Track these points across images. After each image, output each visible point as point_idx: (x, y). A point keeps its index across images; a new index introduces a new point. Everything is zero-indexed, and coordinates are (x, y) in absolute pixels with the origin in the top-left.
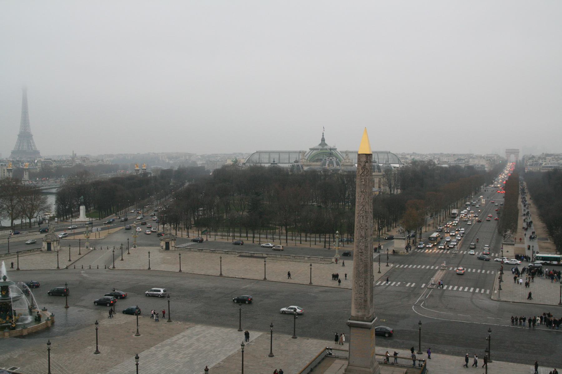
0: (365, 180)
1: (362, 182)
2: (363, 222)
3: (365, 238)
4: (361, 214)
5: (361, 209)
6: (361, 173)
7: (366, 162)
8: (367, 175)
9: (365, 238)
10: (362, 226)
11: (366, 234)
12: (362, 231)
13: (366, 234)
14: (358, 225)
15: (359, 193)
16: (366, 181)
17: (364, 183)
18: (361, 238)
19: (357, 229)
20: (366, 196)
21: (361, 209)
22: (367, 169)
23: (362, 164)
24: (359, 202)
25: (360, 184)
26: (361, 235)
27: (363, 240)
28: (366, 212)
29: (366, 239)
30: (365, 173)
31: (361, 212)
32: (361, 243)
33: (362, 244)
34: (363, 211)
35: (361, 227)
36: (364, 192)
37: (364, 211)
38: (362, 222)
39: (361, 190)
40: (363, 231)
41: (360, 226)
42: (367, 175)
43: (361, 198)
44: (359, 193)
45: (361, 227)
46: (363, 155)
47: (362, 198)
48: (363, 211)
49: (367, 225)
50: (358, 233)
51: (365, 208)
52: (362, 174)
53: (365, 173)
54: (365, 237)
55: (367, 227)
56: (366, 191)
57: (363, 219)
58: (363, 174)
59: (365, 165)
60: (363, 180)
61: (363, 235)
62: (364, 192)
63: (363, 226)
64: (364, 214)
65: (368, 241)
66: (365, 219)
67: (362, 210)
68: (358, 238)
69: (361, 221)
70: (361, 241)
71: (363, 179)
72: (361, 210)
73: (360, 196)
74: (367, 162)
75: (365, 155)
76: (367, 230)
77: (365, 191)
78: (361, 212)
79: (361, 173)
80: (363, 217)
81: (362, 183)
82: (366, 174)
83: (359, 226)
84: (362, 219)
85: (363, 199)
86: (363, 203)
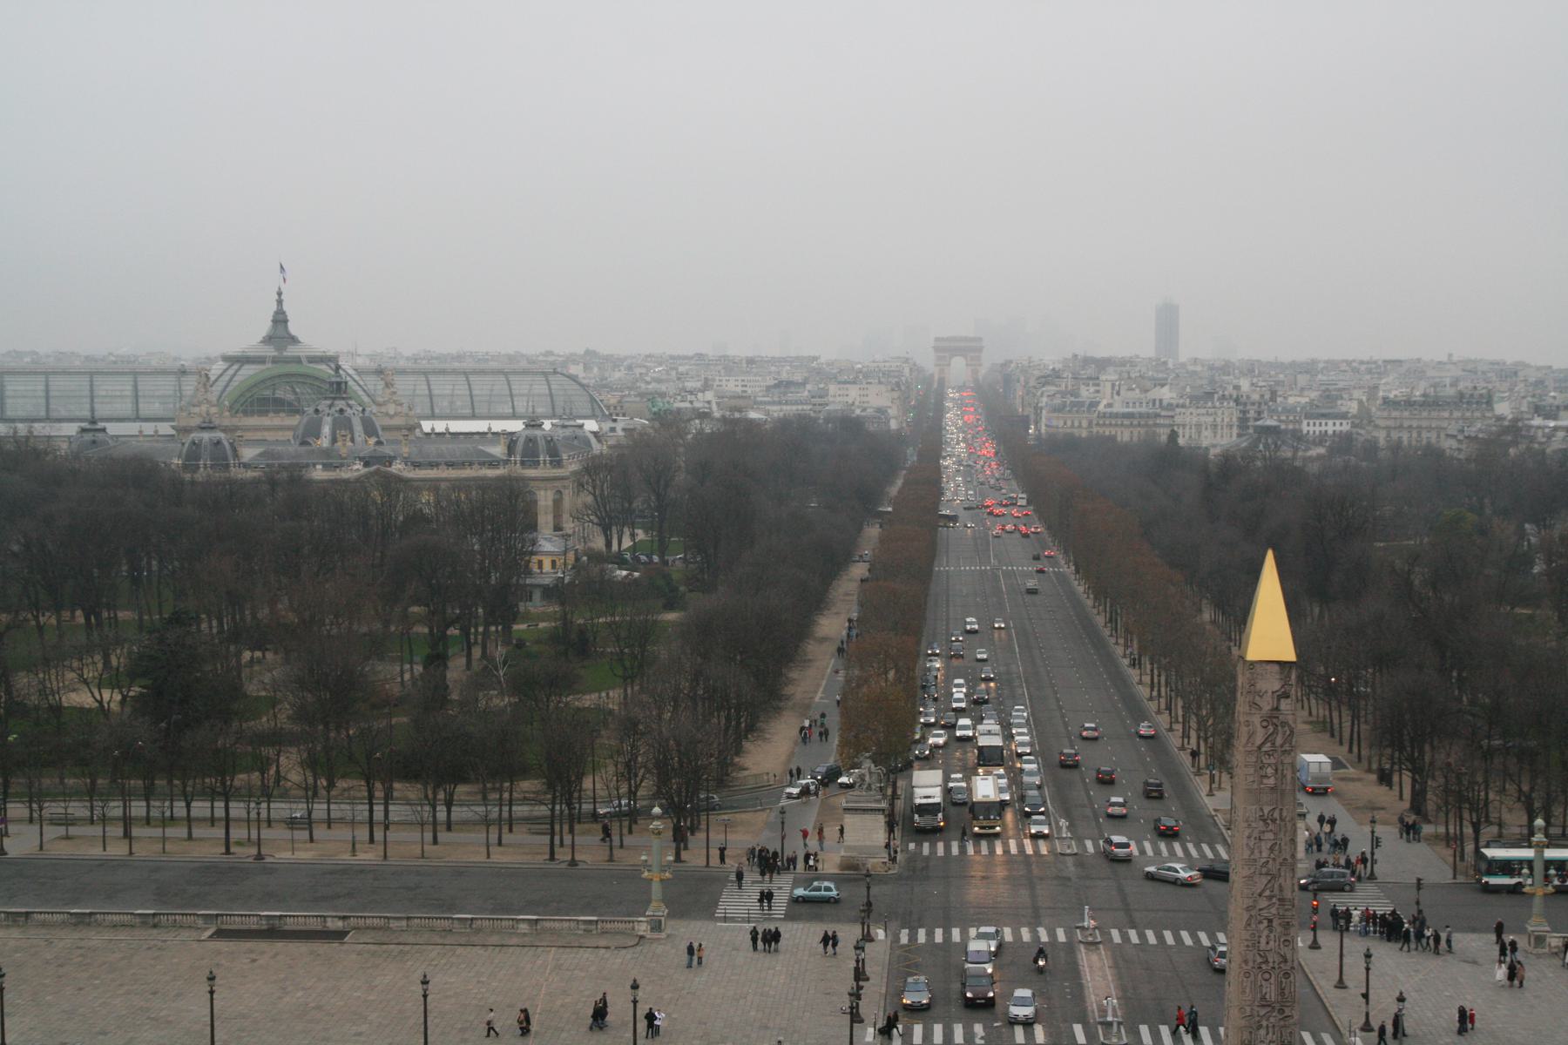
0: (1276, 770)
1: (1266, 776)
2: (1272, 943)
3: (1281, 1011)
4: (1260, 910)
5: (1263, 891)
6: (1259, 740)
7: (1279, 698)
8: (1287, 747)
9: (1281, 1011)
10: (1267, 962)
11: (1282, 994)
12: (1266, 980)
13: (1282, 994)
14: (1250, 957)
15: (1254, 825)
16: (1284, 776)
17: (1271, 781)
18: (1263, 1012)
19: (1247, 974)
20: (1282, 835)
21: (1263, 891)
22: (1284, 724)
23: (1266, 705)
24: (1255, 860)
25: (1255, 786)
26: (1263, 998)
27: (1272, 1020)
28: (1282, 900)
29: (1284, 1011)
30: (1279, 741)
31: (1263, 903)
32: (1263, 1032)
33: (1268, 1034)
34: (1270, 898)
35: (1264, 966)
36: (1274, 821)
37: (1274, 900)
38: (1268, 943)
39: (1262, 810)
40: (1272, 980)
41: (1259, 960)
42: (1287, 747)
43: (1263, 843)
44: (1254, 825)
45: (1264, 966)
46: (1269, 667)
47: (1265, 846)
48: (1270, 898)
49: (1289, 956)
50: (1248, 990)
51: (1280, 886)
52: (1263, 743)
53: (1279, 741)
54: (1277, 1006)
55: (1289, 964)
56: (1284, 814)
57: (1271, 931)
58: (1269, 744)
59: (1277, 709)
60: (1270, 771)
61: (1272, 993)
62: (1274, 821)
63: (1271, 960)
64: (1273, 911)
65: (1291, 1021)
66: (1279, 929)
67: (1267, 893)
68: (1248, 1009)
69: (1263, 940)
70: (1264, 1023)
71: (1269, 765)
72: (1260, 895)
73: (1256, 834)
74: (1286, 696)
75: (1276, 668)
76: (1287, 975)
77: (1276, 815)
78: (1263, 903)
79: (1258, 742)
80: (1270, 921)
81: (1265, 781)
82: (1282, 746)
83: (1254, 961)
84: (1266, 932)
85: (1271, 849)
86: (1270, 866)
